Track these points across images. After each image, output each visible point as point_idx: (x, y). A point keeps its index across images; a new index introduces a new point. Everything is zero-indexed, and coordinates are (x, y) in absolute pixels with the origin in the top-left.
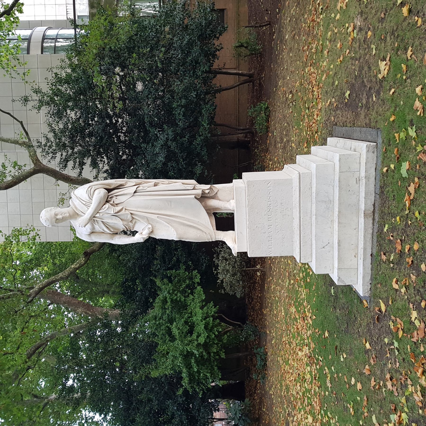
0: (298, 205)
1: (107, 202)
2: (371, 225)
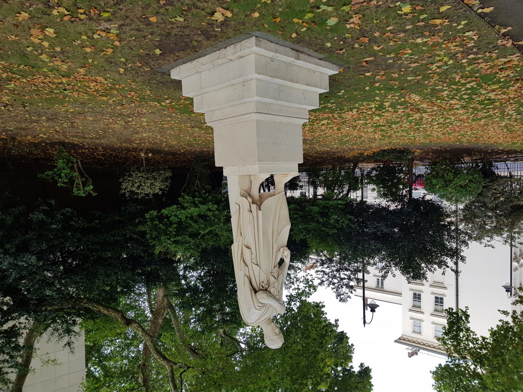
0: (275, 117)
1: (266, 290)
2: (304, 55)
